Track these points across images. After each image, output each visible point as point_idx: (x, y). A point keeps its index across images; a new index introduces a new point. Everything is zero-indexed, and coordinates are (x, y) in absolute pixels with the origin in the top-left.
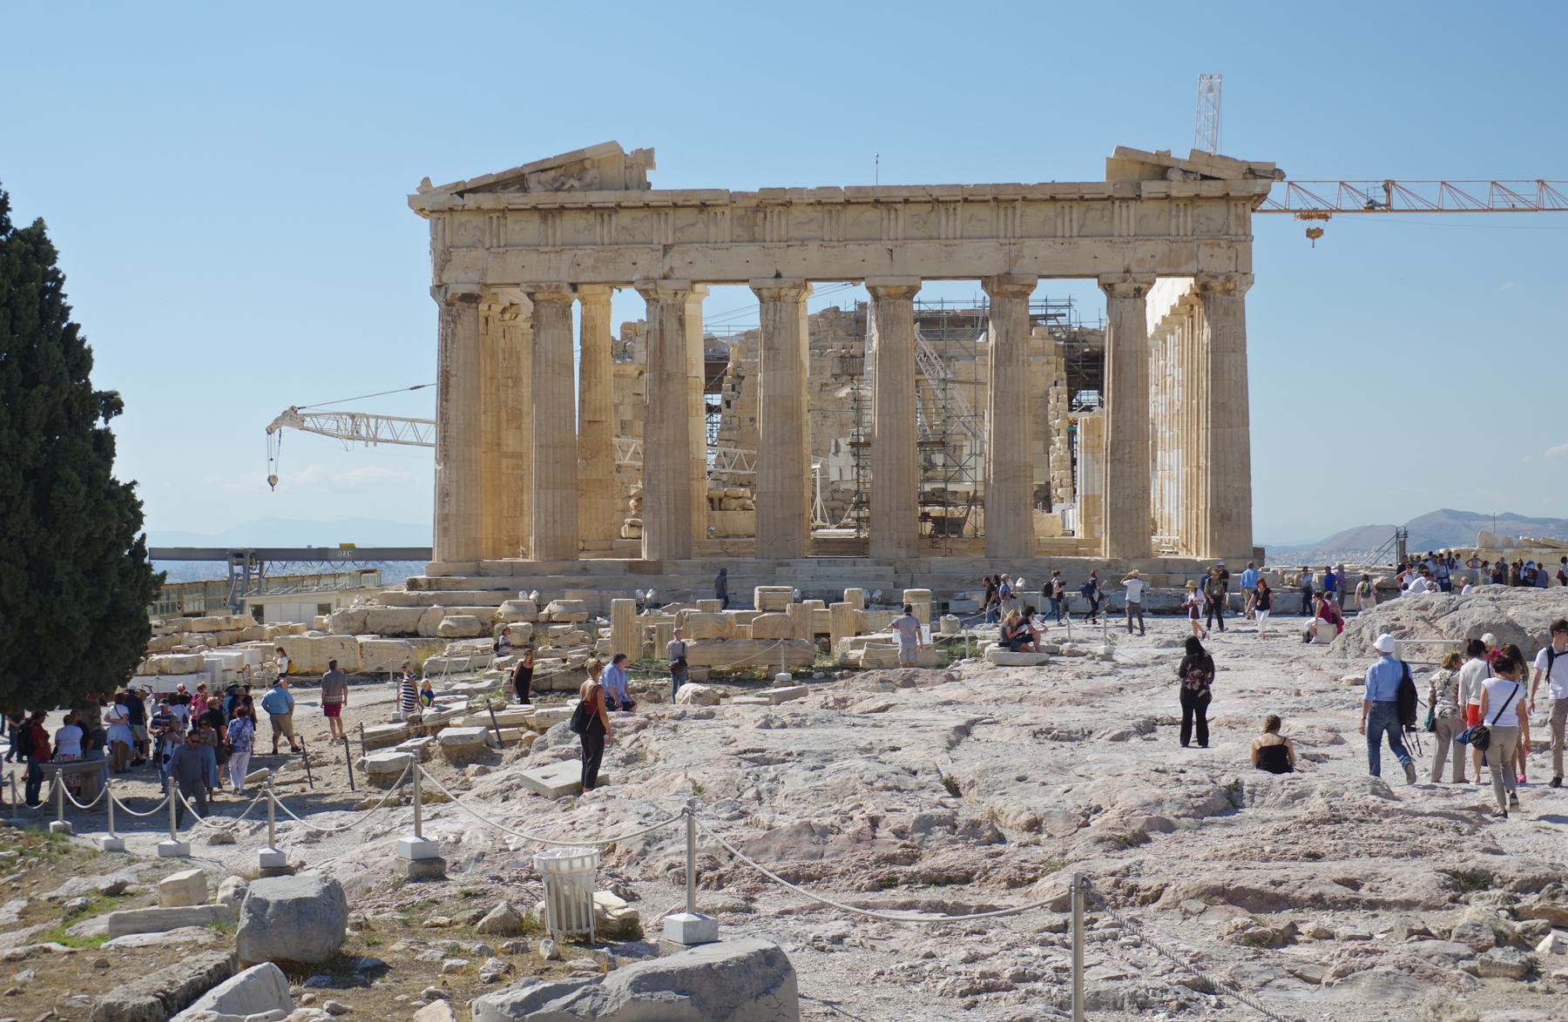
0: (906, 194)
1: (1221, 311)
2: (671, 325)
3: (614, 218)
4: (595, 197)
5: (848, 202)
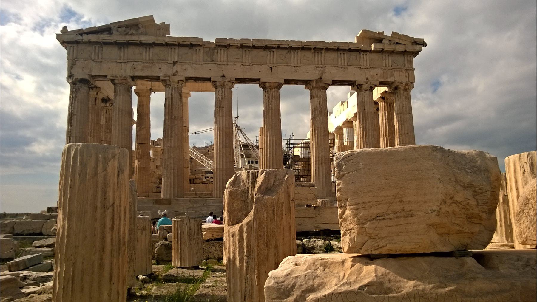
0: (278, 44)
1: (404, 98)
2: (176, 96)
3: (151, 49)
4: (143, 39)
5: (254, 47)
